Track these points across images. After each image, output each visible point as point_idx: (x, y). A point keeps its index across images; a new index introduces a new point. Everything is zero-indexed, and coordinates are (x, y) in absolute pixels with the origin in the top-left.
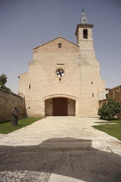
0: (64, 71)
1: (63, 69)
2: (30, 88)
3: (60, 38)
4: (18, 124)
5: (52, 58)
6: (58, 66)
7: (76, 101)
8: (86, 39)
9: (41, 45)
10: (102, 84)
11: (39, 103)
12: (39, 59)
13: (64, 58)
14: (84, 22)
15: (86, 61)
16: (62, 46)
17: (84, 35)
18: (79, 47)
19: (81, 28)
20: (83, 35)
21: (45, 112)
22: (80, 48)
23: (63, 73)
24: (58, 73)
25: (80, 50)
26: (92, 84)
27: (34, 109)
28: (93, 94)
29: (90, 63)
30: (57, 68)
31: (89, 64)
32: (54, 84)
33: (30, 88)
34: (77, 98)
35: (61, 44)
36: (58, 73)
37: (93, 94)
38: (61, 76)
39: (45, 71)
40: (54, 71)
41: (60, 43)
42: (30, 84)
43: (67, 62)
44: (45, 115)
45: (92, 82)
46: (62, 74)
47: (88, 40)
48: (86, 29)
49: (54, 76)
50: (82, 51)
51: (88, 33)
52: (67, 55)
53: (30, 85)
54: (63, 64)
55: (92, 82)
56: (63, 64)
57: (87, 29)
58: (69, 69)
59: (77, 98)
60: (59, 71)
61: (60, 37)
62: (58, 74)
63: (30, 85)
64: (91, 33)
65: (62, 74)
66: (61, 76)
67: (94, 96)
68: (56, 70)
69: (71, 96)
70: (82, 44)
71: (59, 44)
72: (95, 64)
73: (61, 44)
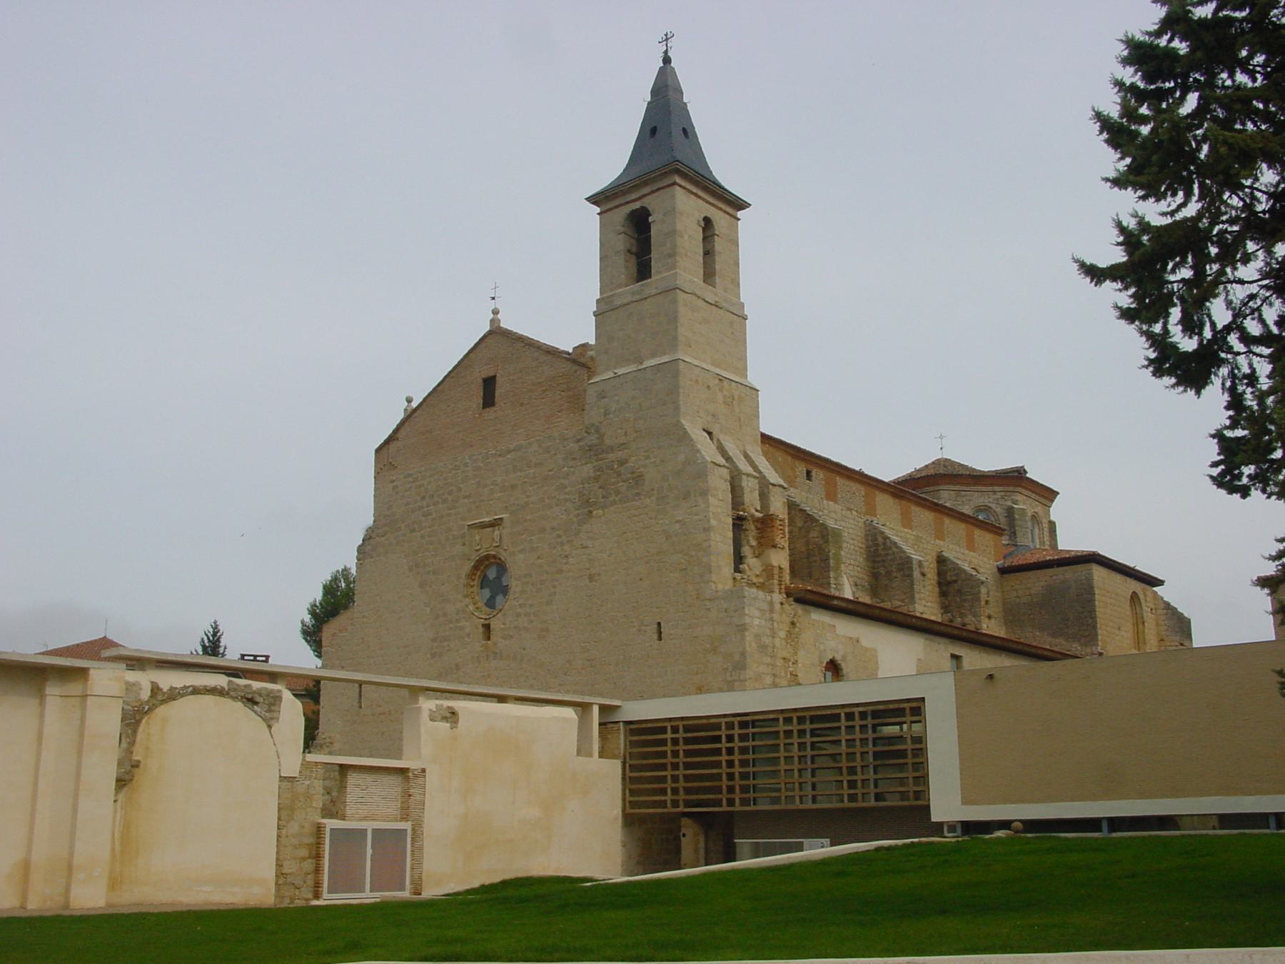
25: (591, 395)
31: (638, 479)
39: (421, 586)
48: (637, 205)
50: (602, 395)
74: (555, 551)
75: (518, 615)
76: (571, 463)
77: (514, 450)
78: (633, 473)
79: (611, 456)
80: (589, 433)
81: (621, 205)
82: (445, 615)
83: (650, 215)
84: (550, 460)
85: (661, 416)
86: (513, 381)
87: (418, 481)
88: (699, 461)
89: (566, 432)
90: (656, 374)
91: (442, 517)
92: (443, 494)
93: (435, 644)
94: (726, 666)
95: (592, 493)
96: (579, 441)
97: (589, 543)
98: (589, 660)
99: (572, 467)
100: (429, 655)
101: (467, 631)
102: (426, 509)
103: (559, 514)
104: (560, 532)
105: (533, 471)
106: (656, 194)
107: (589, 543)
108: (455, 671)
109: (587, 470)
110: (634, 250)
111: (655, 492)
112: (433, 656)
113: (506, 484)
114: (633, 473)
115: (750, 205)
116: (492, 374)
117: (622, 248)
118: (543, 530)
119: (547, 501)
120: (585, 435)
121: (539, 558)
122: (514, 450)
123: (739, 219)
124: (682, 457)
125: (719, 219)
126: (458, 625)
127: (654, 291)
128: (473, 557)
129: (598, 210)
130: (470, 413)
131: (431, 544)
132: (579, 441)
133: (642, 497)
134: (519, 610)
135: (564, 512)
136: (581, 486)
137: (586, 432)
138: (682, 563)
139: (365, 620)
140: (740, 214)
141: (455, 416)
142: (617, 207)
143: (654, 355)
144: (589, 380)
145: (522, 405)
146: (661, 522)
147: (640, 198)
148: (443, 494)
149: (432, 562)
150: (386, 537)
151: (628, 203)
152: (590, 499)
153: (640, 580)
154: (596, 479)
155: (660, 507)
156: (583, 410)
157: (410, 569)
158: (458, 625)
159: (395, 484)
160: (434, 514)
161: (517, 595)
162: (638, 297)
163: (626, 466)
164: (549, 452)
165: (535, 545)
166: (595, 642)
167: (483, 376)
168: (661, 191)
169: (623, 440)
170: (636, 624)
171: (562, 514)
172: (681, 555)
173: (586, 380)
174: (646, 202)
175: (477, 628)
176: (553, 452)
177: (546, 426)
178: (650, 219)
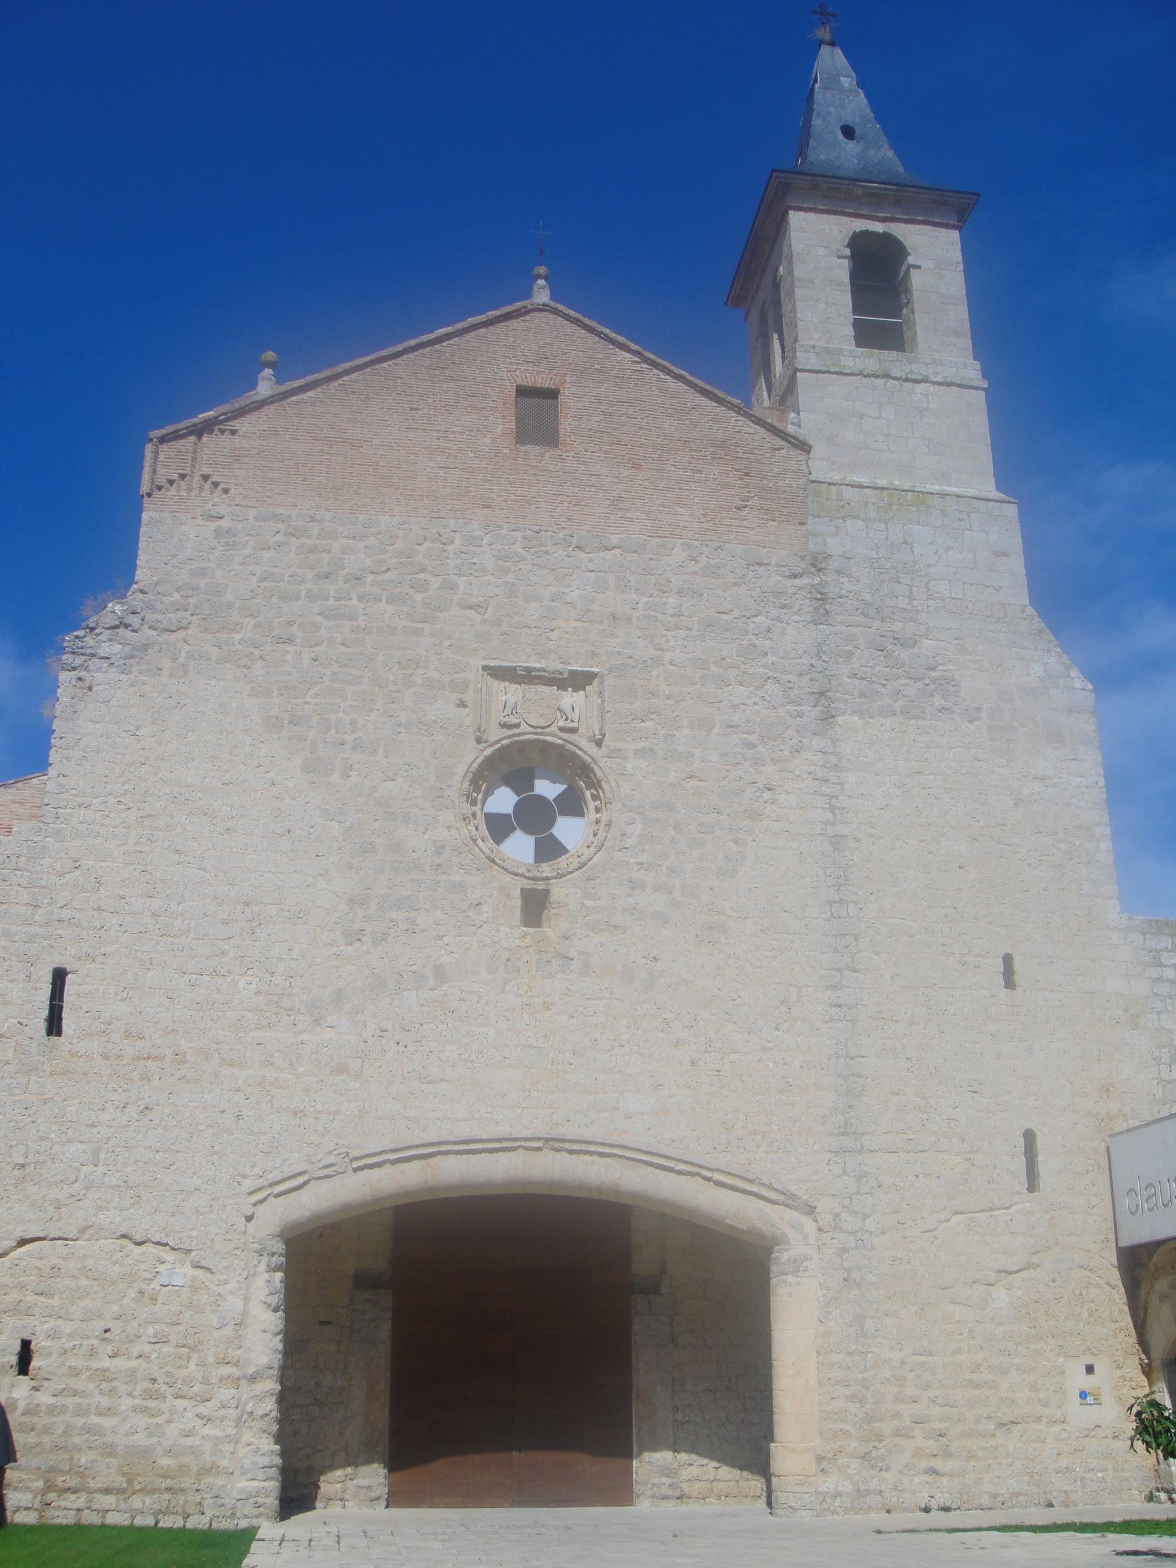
0: (594, 784)
1: (583, 746)
2: (54, 1025)
5: (422, 587)
6: (510, 693)
7: (783, 1256)
8: (892, 355)
11: (184, 1273)
14: (852, 147)
15: (904, 654)
16: (565, 425)
17: (855, 312)
18: (804, 447)
19: (802, 214)
20: (847, 299)
21: (279, 1438)
22: (819, 468)
23: (571, 804)
24: (504, 800)
26: (1009, 983)
27: (103, 1375)
28: (1029, 1137)
30: (495, 734)
33: (54, 1025)
34: (789, 1200)
35: (552, 394)
36: (504, 800)
37: (1029, 1137)
38: (549, 849)
41: (545, 381)
42: (59, 961)
44: (273, 1486)
45: (1008, 960)
46: (566, 829)
47: (918, 370)
48: (878, 227)
49: (440, 849)
51: (917, 280)
53: (59, 977)
54: (578, 681)
55: (1008, 960)
57: (899, 230)
59: (789, 1200)
60: (520, 780)
62: (499, 827)
63: (59, 977)
64: (954, 283)
65: (566, 829)
66: (549, 849)
67: (1045, 1178)
68: (471, 757)
69: (696, 1171)
71: (523, 392)
73: (552, 394)
76: (774, 612)
87: (309, 537)
94: (1157, 1054)
99: (779, 620)
104: (753, 738)
108: (431, 982)
112: (353, 937)
128: (492, 739)
149: (353, 722)
150: (181, 634)
152: (829, 690)
153: (960, 868)
156: (802, 524)
159: (222, 523)
167: (520, 382)
175: (508, 896)
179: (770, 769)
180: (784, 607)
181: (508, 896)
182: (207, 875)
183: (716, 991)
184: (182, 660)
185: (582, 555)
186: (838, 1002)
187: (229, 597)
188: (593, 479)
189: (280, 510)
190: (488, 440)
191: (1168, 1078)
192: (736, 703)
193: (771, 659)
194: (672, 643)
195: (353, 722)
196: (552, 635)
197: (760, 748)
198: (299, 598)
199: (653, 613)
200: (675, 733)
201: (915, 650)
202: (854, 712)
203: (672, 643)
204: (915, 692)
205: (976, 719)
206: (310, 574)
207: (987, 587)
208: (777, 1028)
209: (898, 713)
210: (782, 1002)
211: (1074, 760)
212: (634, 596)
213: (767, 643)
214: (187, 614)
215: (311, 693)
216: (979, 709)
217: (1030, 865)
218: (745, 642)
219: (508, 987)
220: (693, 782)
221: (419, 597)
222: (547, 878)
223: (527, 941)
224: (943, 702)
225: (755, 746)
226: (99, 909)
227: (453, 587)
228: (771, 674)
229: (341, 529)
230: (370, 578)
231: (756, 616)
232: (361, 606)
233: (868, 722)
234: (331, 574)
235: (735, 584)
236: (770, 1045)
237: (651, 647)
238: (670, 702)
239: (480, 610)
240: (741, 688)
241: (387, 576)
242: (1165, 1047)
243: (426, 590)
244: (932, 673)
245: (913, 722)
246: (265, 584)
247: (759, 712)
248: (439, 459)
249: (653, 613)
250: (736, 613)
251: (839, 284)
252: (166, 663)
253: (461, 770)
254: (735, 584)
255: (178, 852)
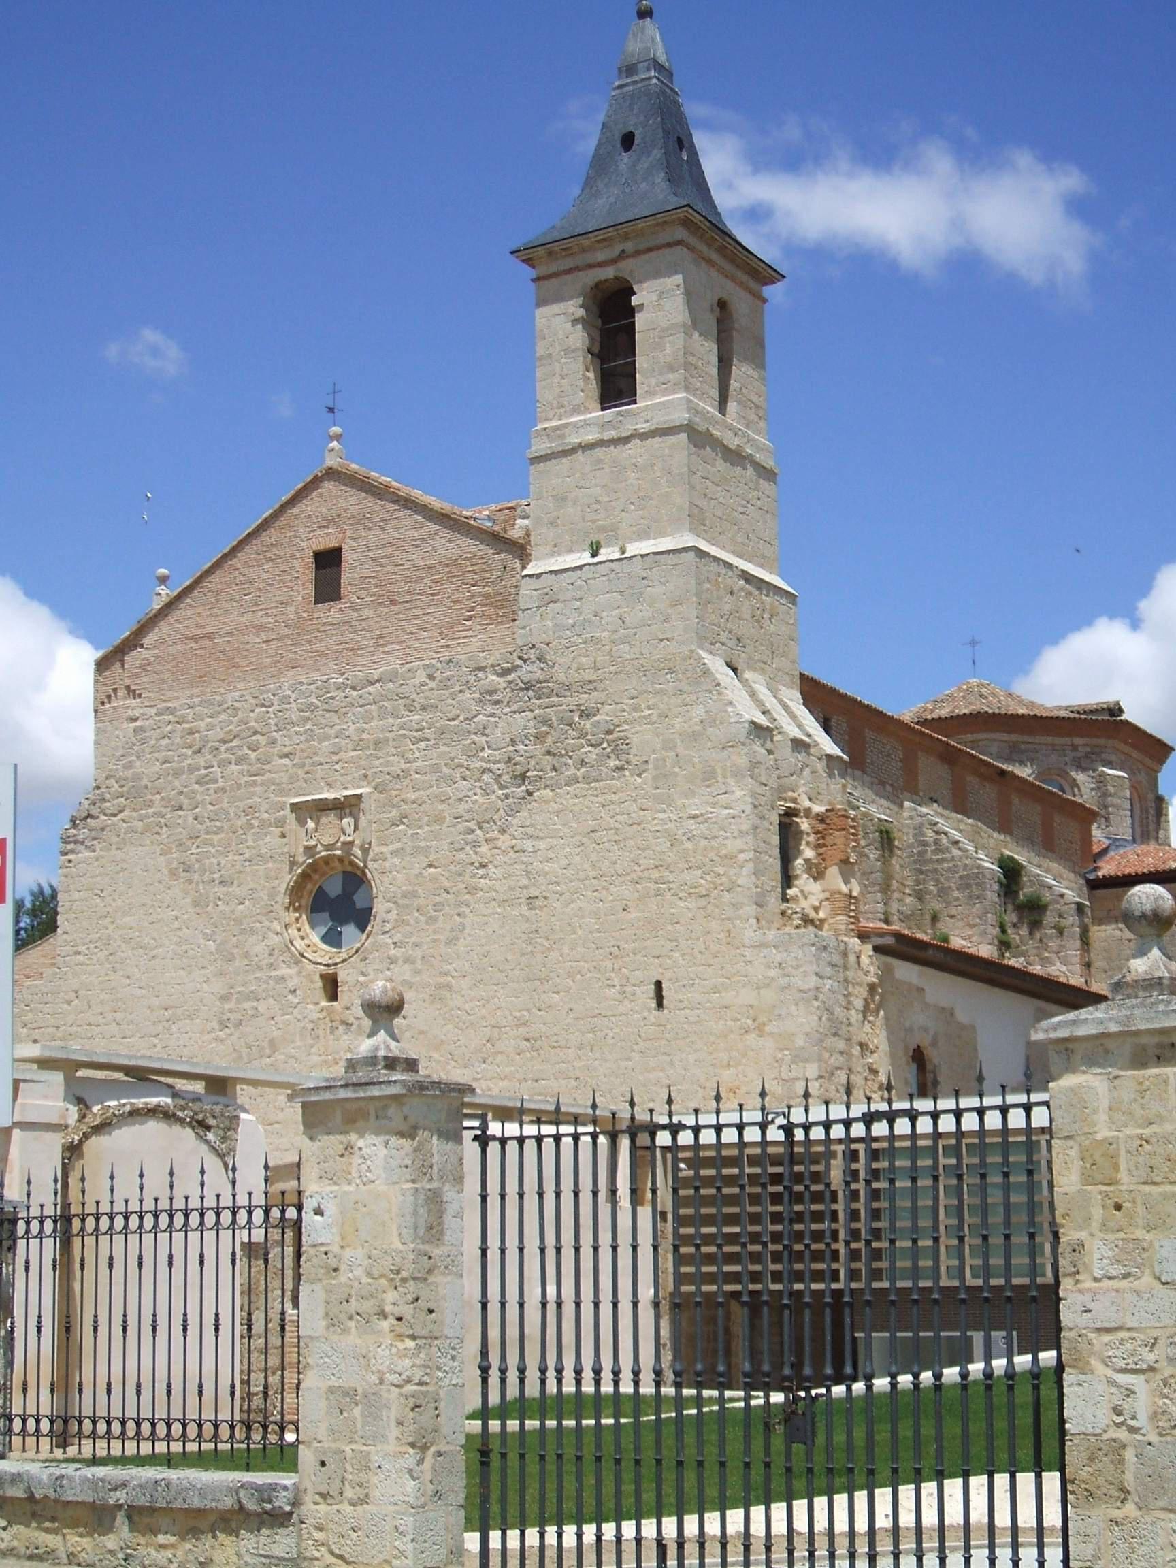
3: (328, 487)
4: (1047, 1125)
9: (157, 606)
10: (769, 996)
12: (137, 777)
13: (368, 719)
15: (588, 725)
25: (528, 593)
29: (641, 738)
31: (619, 747)
32: (272, 1043)
39: (196, 904)
40: (272, 896)
43: (399, 765)
48: (609, 273)
50: (549, 599)
52: (392, 677)
55: (658, 985)
56: (347, 807)
58: (417, 850)
61: (331, 474)
70: (561, 499)
72: (695, 736)
74: (461, 855)
75: (393, 961)
76: (489, 709)
77: (378, 681)
78: (609, 732)
79: (570, 701)
80: (525, 661)
81: (577, 269)
82: (246, 955)
83: (634, 293)
84: (450, 701)
85: (661, 640)
86: (374, 559)
88: (732, 720)
89: (481, 655)
90: (651, 569)
91: (239, 787)
92: (240, 747)
93: (227, 1006)
94: (780, 1056)
95: (533, 762)
96: (505, 672)
97: (528, 845)
98: (528, 1040)
99: (493, 715)
100: (215, 1024)
101: (291, 984)
102: (203, 772)
103: (470, 793)
104: (472, 825)
105: (417, 717)
106: (646, 257)
107: (528, 845)
108: (268, 1051)
109: (522, 722)
110: (596, 350)
111: (650, 766)
112: (223, 1025)
113: (365, 736)
114: (609, 732)
115: (784, 277)
116: (333, 544)
117: (579, 344)
118: (439, 819)
119: (446, 770)
120: (519, 662)
121: (431, 866)
122: (378, 681)
123: (765, 301)
124: (699, 712)
125: (741, 304)
126: (273, 973)
127: (643, 427)
129: (532, 273)
130: (292, 609)
131: (216, 833)
132: (505, 672)
133: (627, 773)
134: (392, 952)
135: (479, 791)
136: (511, 748)
137: (520, 658)
138: (701, 886)
139: (80, 958)
140: (767, 291)
141: (260, 613)
142: (570, 271)
143: (643, 535)
144: (524, 567)
145: (393, 602)
146: (661, 816)
147: (613, 261)
148: (240, 747)
149: (219, 864)
150: (120, 816)
151: (590, 266)
153: (624, 910)
154: (539, 738)
155: (658, 791)
156: (514, 620)
157: (173, 873)
158: (273, 973)
159: (138, 724)
160: (220, 780)
161: (388, 926)
162: (614, 434)
163: (596, 718)
164: (447, 687)
165: (423, 844)
166: (540, 1010)
167: (315, 548)
168: (653, 254)
169: (589, 675)
170: (616, 983)
171: (475, 794)
172: (699, 872)
173: (519, 570)
174: (626, 268)
175: (312, 982)
176: (458, 688)
177: (443, 643)
178: (635, 300)
179: (484, 849)
180: (497, 702)
181: (312, 982)
182: (143, 991)
183: (443, 1037)
184: (122, 835)
185: (355, 693)
186: (527, 1036)
187: (145, 782)
188: (363, 623)
189: (169, 704)
190: (292, 609)
191: (787, 1078)
192: (461, 796)
193: (487, 752)
194: (417, 754)
195: (219, 864)
196: (337, 767)
197: (479, 832)
198: (183, 773)
199: (404, 732)
200: (419, 831)
201: (596, 718)
202: (546, 786)
203: (417, 754)
204: (595, 757)
205: (644, 772)
206: (189, 752)
207: (661, 640)
208: (484, 1062)
209: (580, 779)
210: (488, 1041)
211: (725, 793)
212: (391, 721)
213: (484, 738)
214: (123, 799)
215: (195, 846)
216: (646, 762)
217: (680, 899)
218: (468, 742)
219: (313, 1050)
220: (432, 870)
221: (253, 755)
222: (336, 964)
223: (324, 1013)
224: (617, 762)
225: (473, 831)
226: (90, 1024)
227: (274, 742)
228: (484, 765)
229: (206, 711)
230: (223, 748)
231: (476, 716)
232: (219, 770)
233: (557, 793)
234: (201, 749)
235: (461, 691)
236: (480, 1076)
237: (402, 761)
238: (415, 805)
239: (291, 757)
240: (465, 782)
241: (234, 744)
242: (787, 1049)
243: (258, 748)
244: (611, 737)
245: (593, 785)
246: (164, 766)
247: (476, 801)
248: (263, 634)
249: (404, 732)
250: (461, 718)
251: (573, 351)
252: (114, 839)
253: (283, 888)
254: (461, 691)
255: (128, 977)
